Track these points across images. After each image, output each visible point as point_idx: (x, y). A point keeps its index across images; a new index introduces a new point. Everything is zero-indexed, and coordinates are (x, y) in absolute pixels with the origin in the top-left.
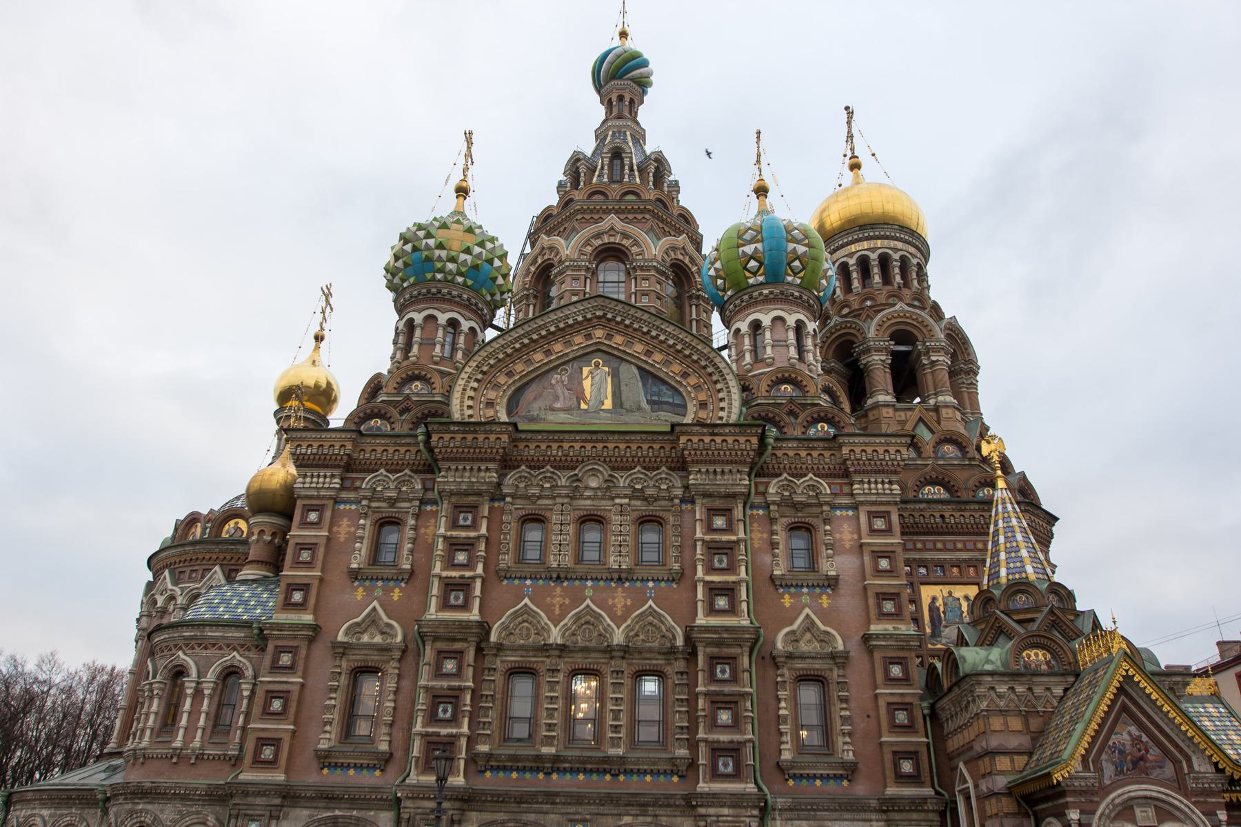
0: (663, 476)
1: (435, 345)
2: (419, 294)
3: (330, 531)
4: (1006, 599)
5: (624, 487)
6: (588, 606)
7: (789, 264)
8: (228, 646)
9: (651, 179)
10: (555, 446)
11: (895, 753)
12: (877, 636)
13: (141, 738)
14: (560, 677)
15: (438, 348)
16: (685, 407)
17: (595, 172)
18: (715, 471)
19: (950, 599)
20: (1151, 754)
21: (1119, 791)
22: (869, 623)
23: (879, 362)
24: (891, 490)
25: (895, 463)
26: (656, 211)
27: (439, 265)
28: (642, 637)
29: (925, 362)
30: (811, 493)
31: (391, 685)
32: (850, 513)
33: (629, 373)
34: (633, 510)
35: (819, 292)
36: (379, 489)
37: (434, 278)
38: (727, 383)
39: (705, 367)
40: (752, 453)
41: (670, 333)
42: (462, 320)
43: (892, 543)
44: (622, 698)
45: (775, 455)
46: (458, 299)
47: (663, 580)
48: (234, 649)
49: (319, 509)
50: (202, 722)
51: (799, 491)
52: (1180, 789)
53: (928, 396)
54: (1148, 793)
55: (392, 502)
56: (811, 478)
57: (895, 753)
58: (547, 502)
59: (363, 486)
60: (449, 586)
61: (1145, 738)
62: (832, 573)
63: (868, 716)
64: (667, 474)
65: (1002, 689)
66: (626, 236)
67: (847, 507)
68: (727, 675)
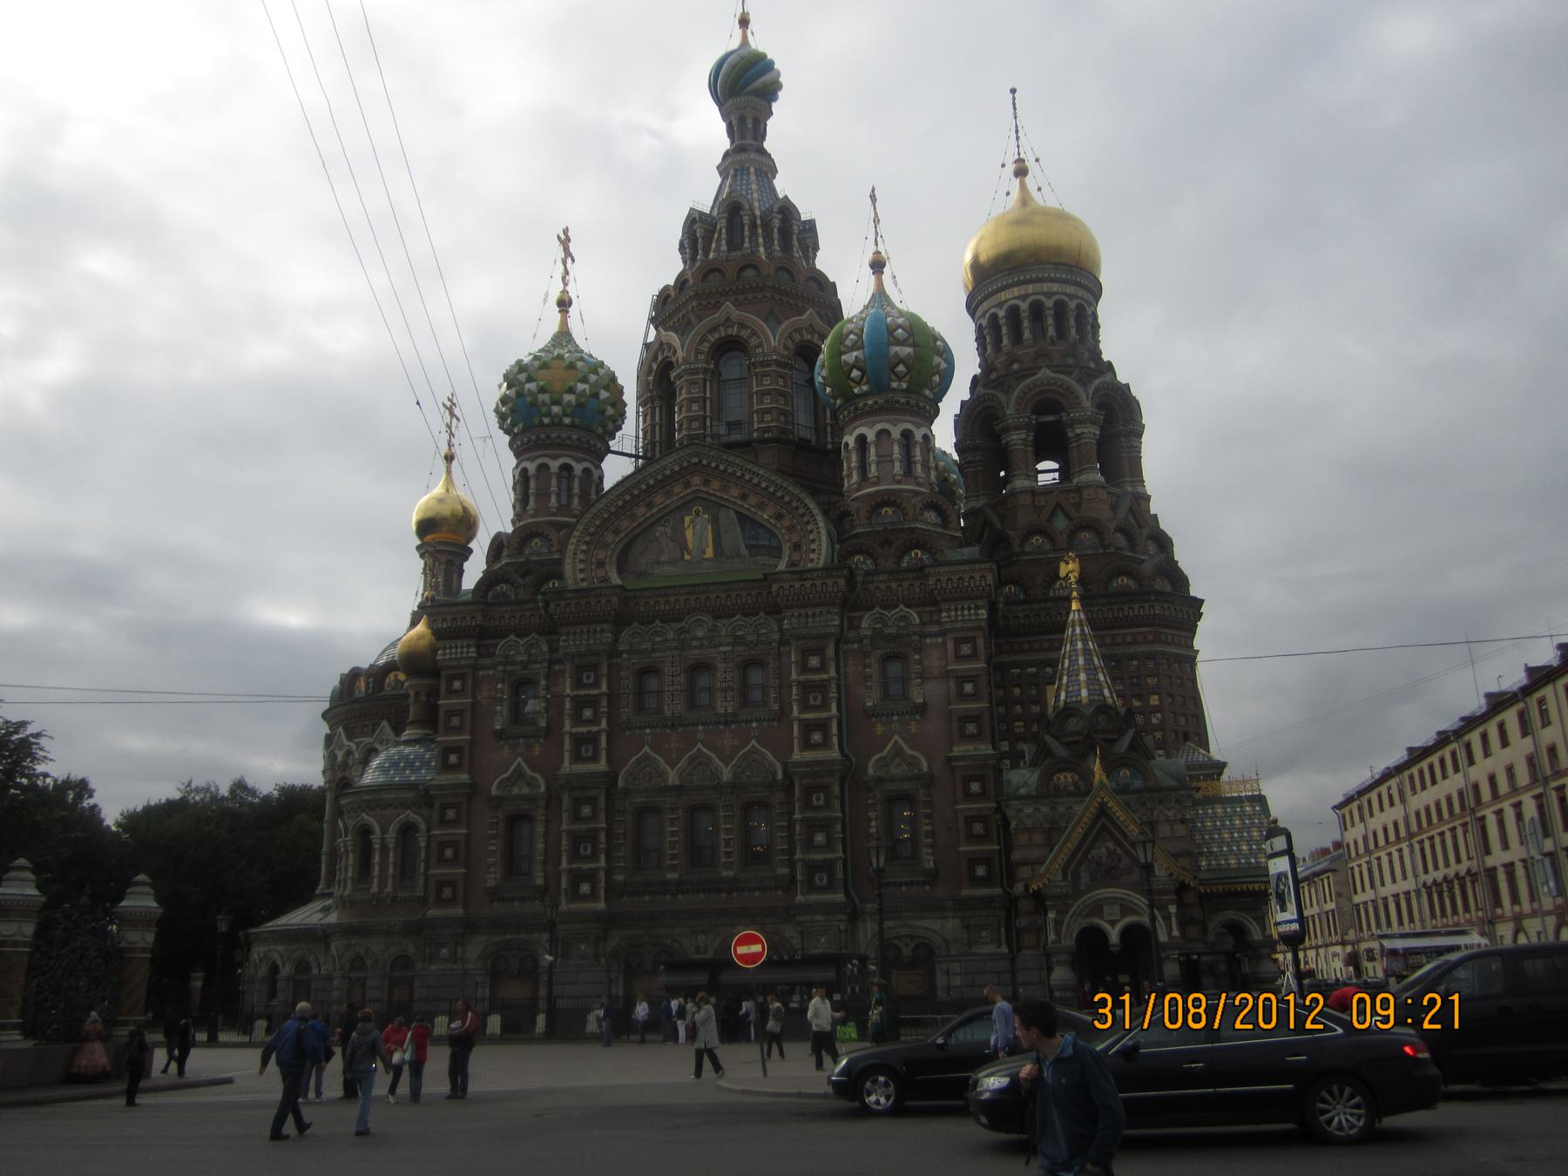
0: (762, 621)
1: (550, 495)
2: (530, 441)
3: (474, 696)
5: (726, 636)
6: (699, 749)
7: (892, 369)
8: (402, 805)
9: (776, 236)
10: (662, 600)
12: (957, 758)
13: (345, 887)
14: (681, 812)
15: (553, 499)
16: (780, 548)
17: (714, 232)
18: (807, 615)
21: (1090, 895)
23: (1019, 442)
24: (976, 614)
25: (980, 588)
26: (777, 286)
27: (544, 410)
28: (748, 773)
29: (1070, 435)
30: (902, 624)
31: (540, 829)
32: (940, 640)
33: (728, 517)
35: (931, 389)
36: (512, 653)
37: (541, 424)
38: (817, 524)
39: (797, 508)
40: (840, 594)
41: (762, 476)
42: (574, 464)
44: (732, 829)
45: (867, 589)
46: (568, 442)
47: (765, 719)
48: (408, 808)
49: (462, 677)
50: (391, 871)
51: (890, 623)
53: (1074, 473)
54: (1114, 895)
55: (525, 665)
56: (901, 610)
58: (658, 654)
59: (497, 652)
60: (579, 741)
61: (1119, 851)
62: (921, 700)
65: (1029, 810)
66: (742, 326)
67: (936, 635)
68: (822, 802)
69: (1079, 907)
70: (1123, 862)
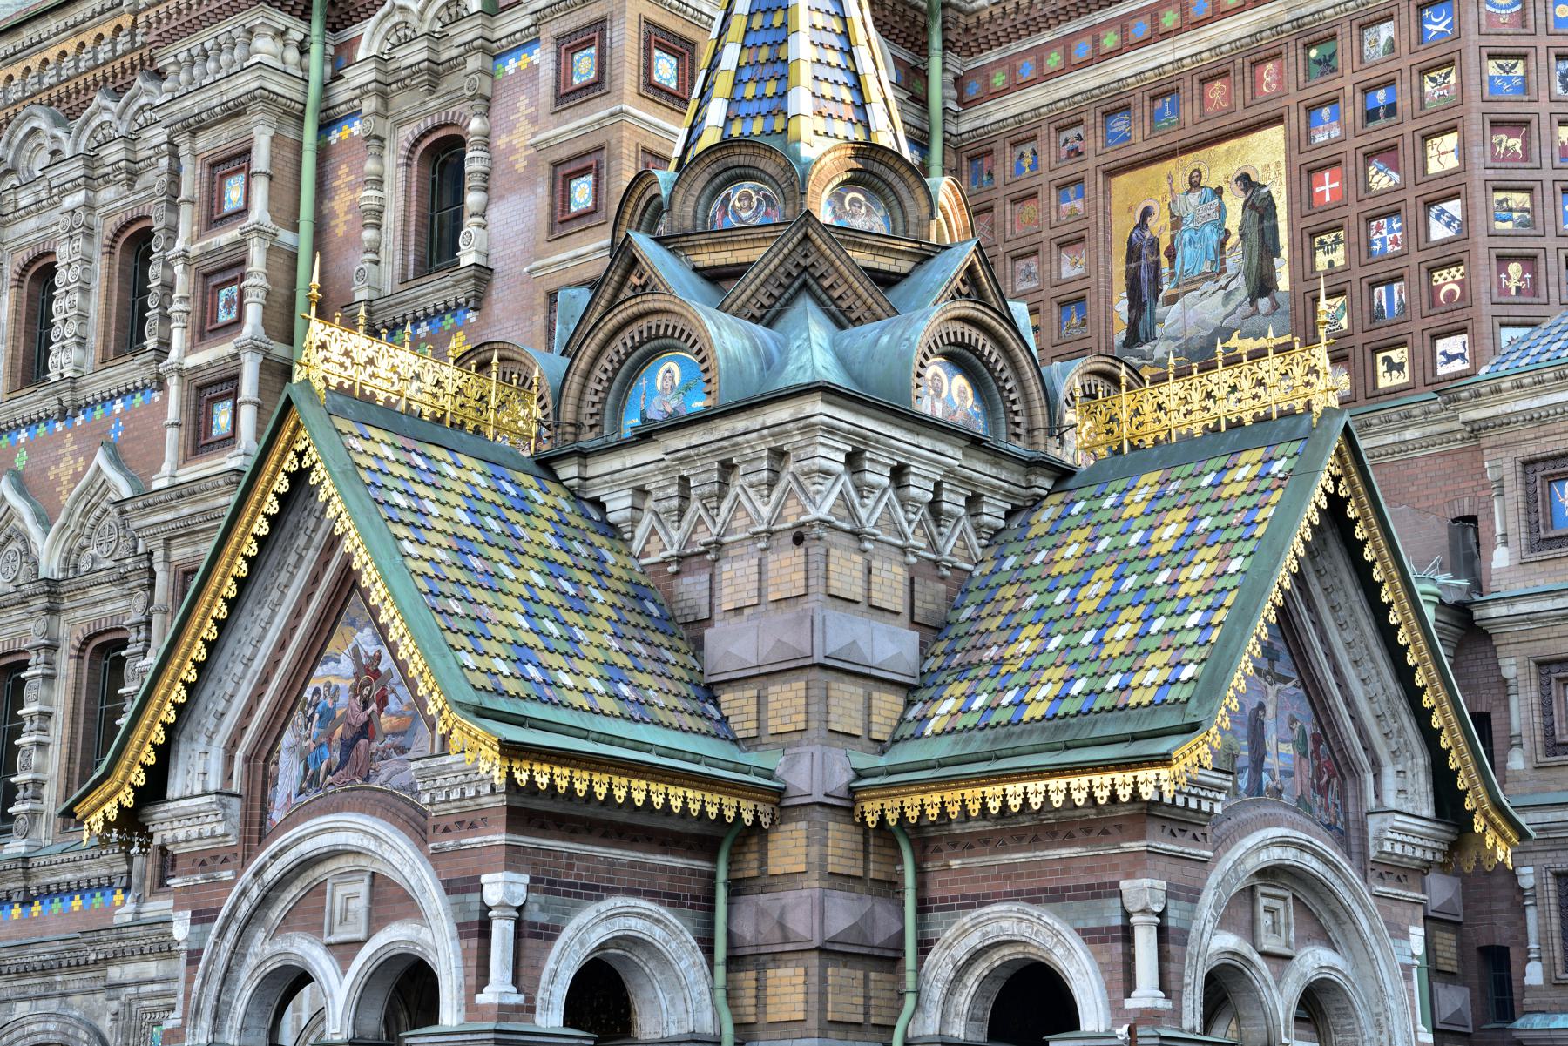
0: (143, 100)
19: (1194, 198)
21: (274, 846)
34: (107, 216)
43: (598, 121)
64: (148, 92)
69: (243, 893)
70: (393, 704)
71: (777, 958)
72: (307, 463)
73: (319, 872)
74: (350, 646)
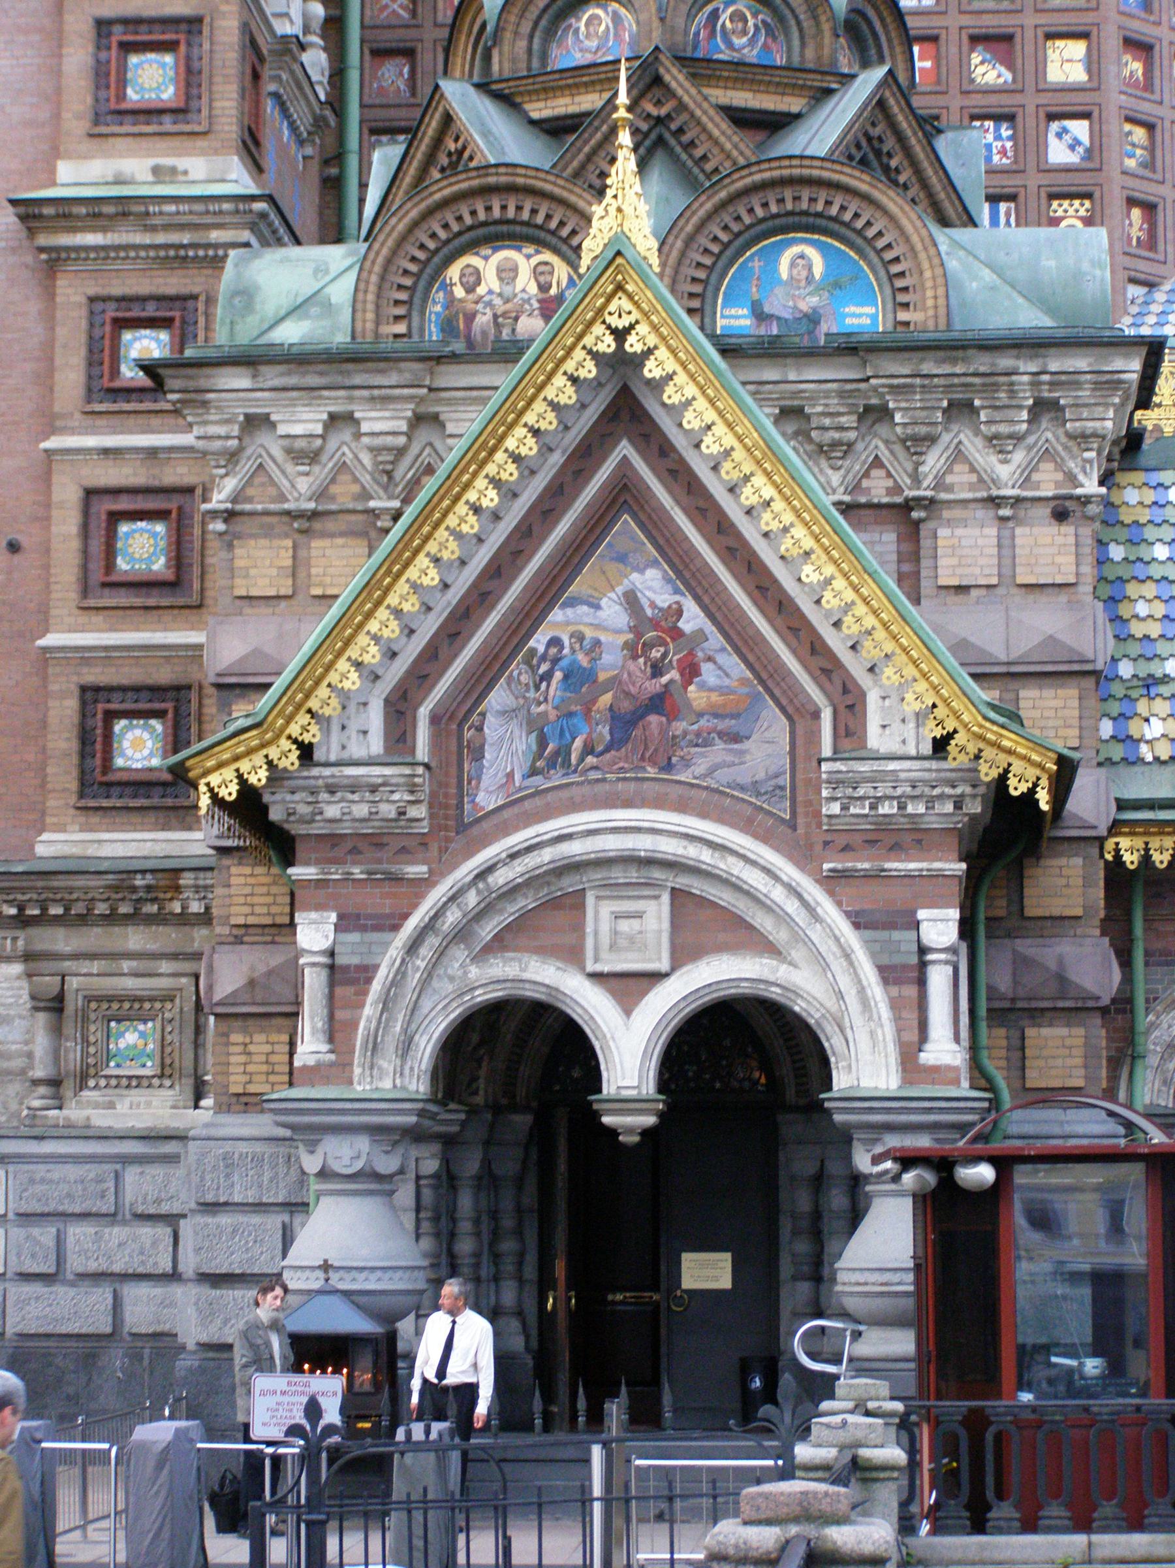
4: (526, 27)
11: (90, 694)
20: (703, 686)
22: (55, 152)
52: (794, 828)
54: (643, 844)
57: (90, 694)
61: (693, 619)
63: (14, 547)
69: (452, 899)
70: (709, 674)
71: (1037, 1015)
72: (633, 344)
73: (569, 883)
74: (620, 590)
